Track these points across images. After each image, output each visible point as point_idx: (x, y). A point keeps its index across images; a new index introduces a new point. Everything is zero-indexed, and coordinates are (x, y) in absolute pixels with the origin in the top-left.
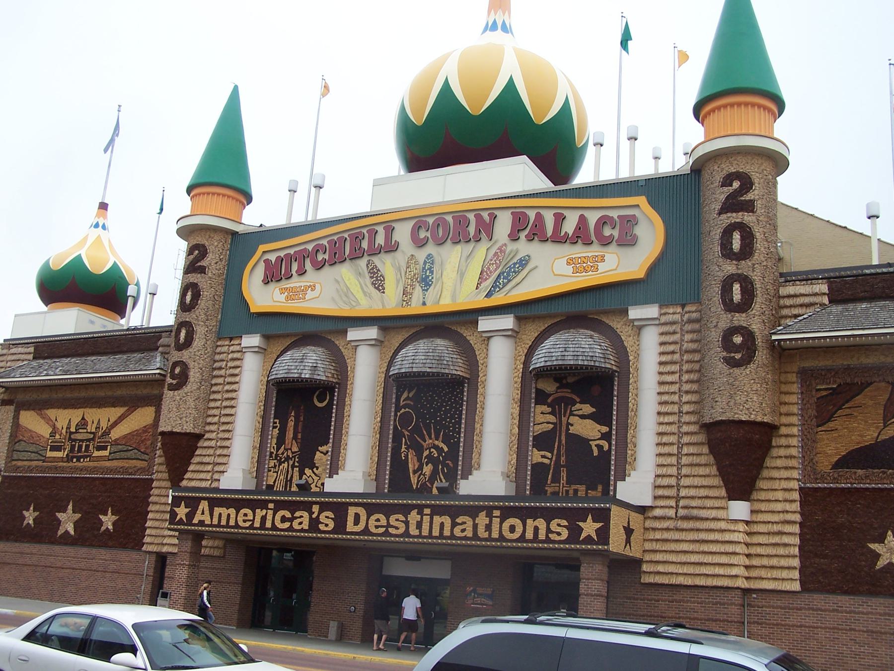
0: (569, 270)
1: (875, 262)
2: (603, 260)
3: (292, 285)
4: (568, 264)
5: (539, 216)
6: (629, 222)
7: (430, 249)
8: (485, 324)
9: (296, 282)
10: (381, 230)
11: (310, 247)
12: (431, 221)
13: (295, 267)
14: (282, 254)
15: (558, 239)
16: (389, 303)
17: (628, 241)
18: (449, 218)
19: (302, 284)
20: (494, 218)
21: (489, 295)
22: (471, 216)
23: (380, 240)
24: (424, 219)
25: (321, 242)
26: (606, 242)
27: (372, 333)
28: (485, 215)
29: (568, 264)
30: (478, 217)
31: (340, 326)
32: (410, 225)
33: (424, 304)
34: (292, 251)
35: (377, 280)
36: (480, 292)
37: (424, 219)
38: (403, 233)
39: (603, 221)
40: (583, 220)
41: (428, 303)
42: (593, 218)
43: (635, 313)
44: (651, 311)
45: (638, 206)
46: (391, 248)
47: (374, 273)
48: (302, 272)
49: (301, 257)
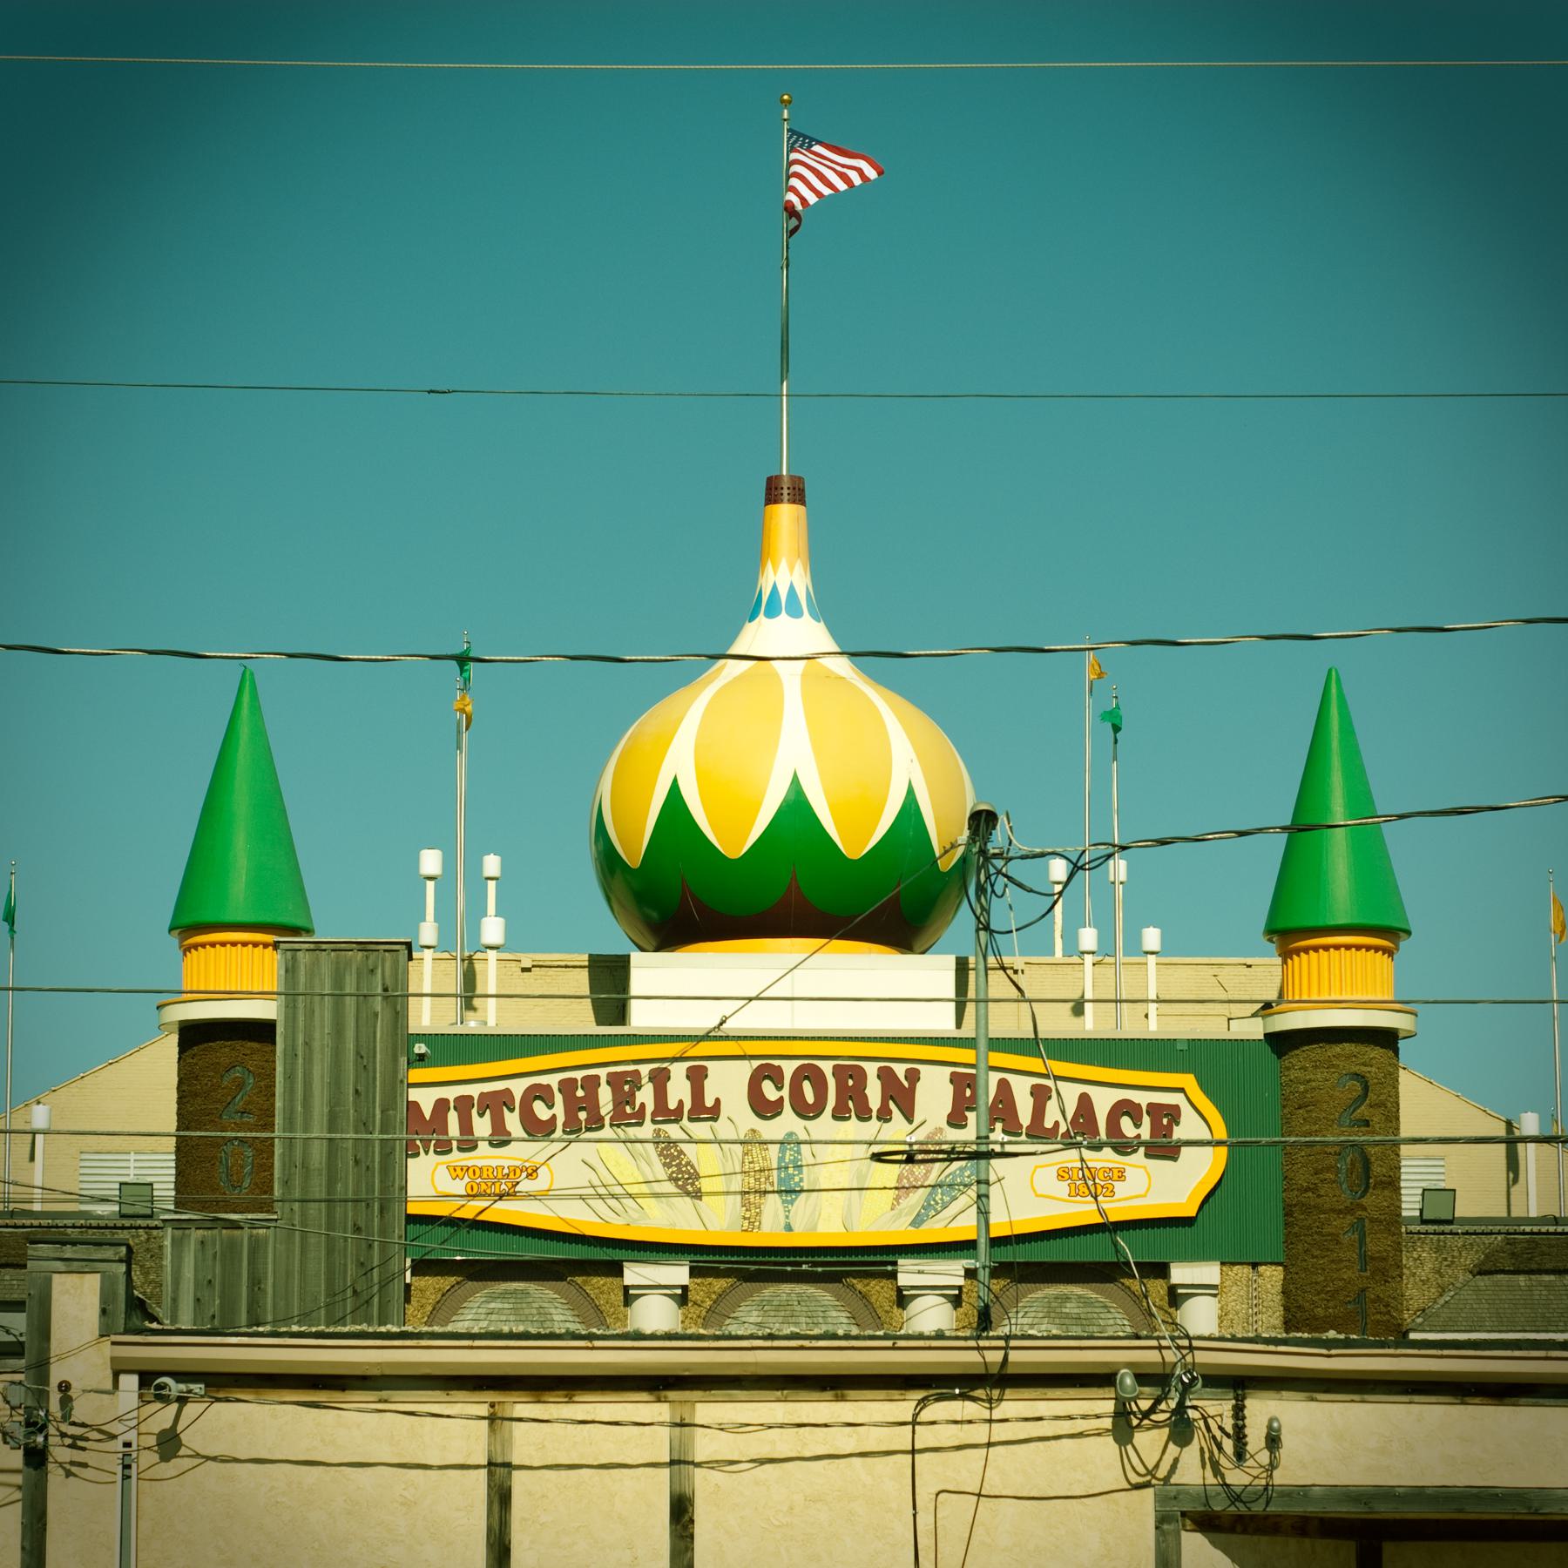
0: (1063, 1188)
1: (1533, 1214)
2: (1122, 1176)
3: (469, 1163)
4: (1060, 1177)
5: (1004, 1086)
6: (1166, 1116)
7: (788, 1122)
8: (910, 1273)
9: (485, 1156)
10: (678, 1071)
11: (518, 1088)
12: (788, 1068)
13: (482, 1126)
14: (451, 1093)
15: (1038, 1132)
16: (716, 1221)
17: (1164, 1149)
18: (827, 1067)
19: (506, 1163)
20: (913, 1076)
21: (917, 1222)
22: (871, 1069)
23: (679, 1090)
24: (776, 1063)
25: (543, 1080)
26: (1123, 1147)
27: (678, 1274)
28: (900, 1070)
29: (1060, 1177)
30: (886, 1076)
31: (616, 1255)
32: (746, 1069)
33: (789, 1228)
34: (474, 1091)
35: (679, 1171)
36: (900, 1215)
37: (776, 1063)
38: (728, 1083)
39: (1124, 1108)
40: (1085, 1102)
41: (797, 1227)
42: (1103, 1102)
43: (1181, 1274)
44: (1209, 1272)
45: (1182, 1090)
46: (705, 1111)
47: (673, 1158)
48: (500, 1139)
49: (496, 1104)
